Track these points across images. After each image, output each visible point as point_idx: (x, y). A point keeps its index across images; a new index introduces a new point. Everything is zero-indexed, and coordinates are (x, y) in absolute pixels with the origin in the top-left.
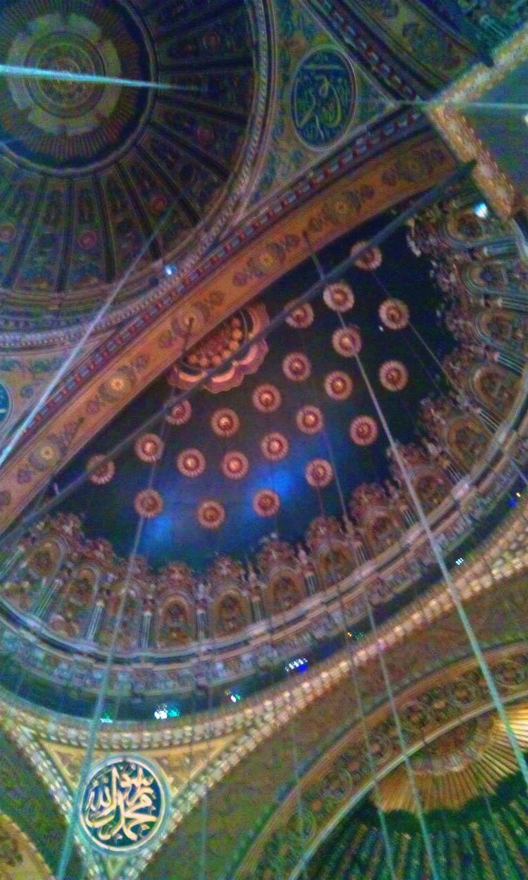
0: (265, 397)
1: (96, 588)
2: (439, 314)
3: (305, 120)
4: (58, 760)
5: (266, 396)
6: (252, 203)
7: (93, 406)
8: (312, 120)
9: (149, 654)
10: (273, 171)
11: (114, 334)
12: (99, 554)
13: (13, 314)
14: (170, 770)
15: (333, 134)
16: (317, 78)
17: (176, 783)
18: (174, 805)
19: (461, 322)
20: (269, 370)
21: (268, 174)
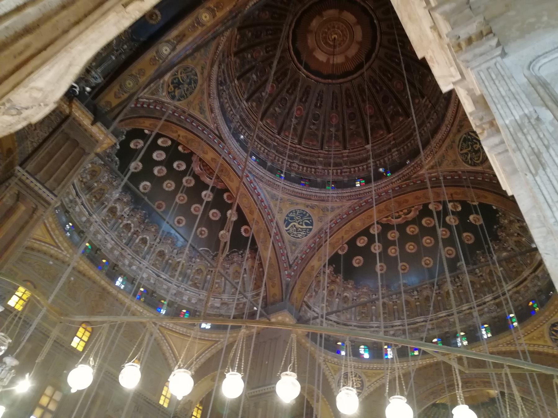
0: (411, 230)
1: (336, 293)
2: (495, 227)
3: (465, 151)
4: (330, 368)
5: (412, 229)
6: (430, 169)
7: (347, 232)
8: (467, 154)
9: (355, 324)
10: (442, 161)
11: (359, 201)
12: (338, 280)
13: (304, 161)
14: (367, 376)
15: (475, 165)
16: (474, 141)
17: (369, 381)
18: (368, 387)
19: (504, 234)
20: (416, 221)
21: (440, 160)
